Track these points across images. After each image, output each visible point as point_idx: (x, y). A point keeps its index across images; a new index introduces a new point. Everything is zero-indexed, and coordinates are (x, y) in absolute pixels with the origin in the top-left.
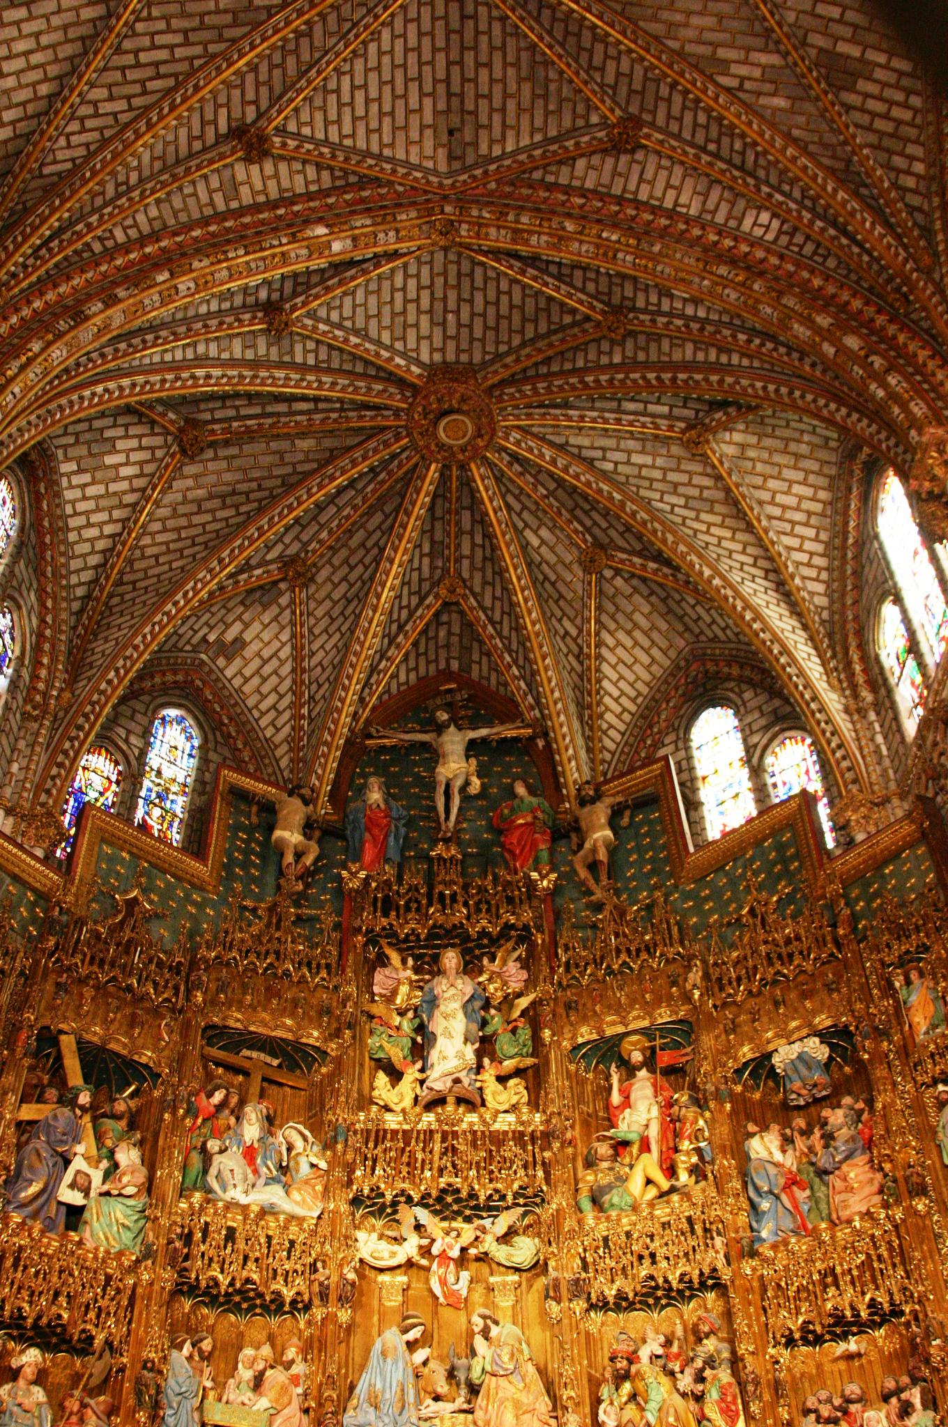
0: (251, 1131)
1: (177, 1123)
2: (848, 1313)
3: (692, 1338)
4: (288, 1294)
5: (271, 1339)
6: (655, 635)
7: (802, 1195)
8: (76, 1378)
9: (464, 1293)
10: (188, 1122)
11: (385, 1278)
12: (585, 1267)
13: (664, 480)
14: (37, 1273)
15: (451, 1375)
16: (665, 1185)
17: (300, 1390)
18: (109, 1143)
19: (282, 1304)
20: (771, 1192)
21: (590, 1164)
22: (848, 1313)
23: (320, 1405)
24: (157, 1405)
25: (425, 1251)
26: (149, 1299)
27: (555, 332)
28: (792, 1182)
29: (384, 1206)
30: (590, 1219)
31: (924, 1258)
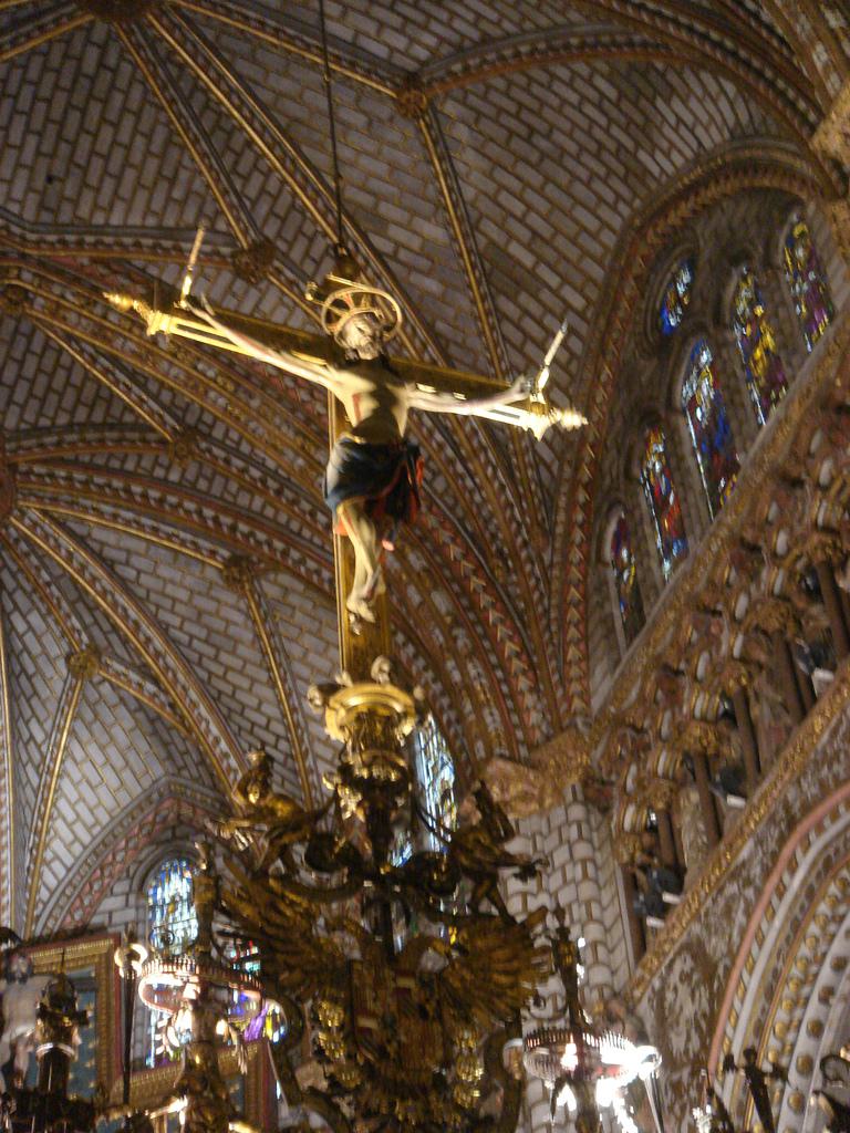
6: (132, 757)
13: (188, 603)
27: (112, 427)
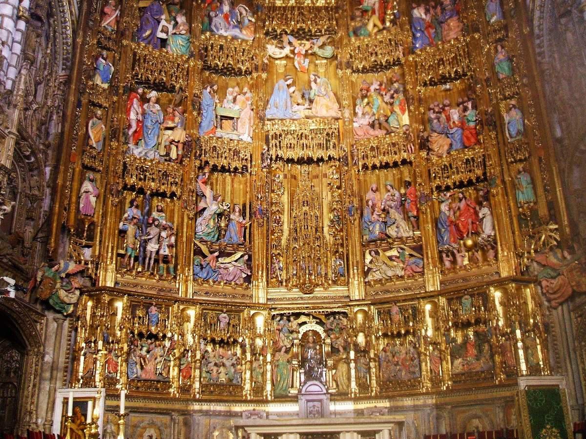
0: (226, 8)
1: (199, 5)
2: (447, 75)
3: (389, 83)
4: (244, 68)
5: (238, 84)
7: (432, 31)
8: (170, 101)
9: (307, 67)
10: (202, 5)
11: (277, 62)
12: (351, 57)
14: (153, 64)
15: (303, 96)
16: (381, 27)
17: (250, 103)
18: (174, 14)
19: (242, 72)
20: (420, 30)
21: (353, 18)
22: (447, 75)
23: (257, 107)
24: (200, 109)
25: (293, 52)
26: (194, 71)
28: (429, 26)
29: (276, 35)
30: (353, 39)
31: (476, 56)
